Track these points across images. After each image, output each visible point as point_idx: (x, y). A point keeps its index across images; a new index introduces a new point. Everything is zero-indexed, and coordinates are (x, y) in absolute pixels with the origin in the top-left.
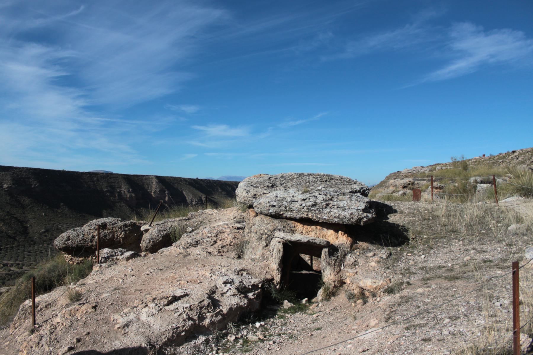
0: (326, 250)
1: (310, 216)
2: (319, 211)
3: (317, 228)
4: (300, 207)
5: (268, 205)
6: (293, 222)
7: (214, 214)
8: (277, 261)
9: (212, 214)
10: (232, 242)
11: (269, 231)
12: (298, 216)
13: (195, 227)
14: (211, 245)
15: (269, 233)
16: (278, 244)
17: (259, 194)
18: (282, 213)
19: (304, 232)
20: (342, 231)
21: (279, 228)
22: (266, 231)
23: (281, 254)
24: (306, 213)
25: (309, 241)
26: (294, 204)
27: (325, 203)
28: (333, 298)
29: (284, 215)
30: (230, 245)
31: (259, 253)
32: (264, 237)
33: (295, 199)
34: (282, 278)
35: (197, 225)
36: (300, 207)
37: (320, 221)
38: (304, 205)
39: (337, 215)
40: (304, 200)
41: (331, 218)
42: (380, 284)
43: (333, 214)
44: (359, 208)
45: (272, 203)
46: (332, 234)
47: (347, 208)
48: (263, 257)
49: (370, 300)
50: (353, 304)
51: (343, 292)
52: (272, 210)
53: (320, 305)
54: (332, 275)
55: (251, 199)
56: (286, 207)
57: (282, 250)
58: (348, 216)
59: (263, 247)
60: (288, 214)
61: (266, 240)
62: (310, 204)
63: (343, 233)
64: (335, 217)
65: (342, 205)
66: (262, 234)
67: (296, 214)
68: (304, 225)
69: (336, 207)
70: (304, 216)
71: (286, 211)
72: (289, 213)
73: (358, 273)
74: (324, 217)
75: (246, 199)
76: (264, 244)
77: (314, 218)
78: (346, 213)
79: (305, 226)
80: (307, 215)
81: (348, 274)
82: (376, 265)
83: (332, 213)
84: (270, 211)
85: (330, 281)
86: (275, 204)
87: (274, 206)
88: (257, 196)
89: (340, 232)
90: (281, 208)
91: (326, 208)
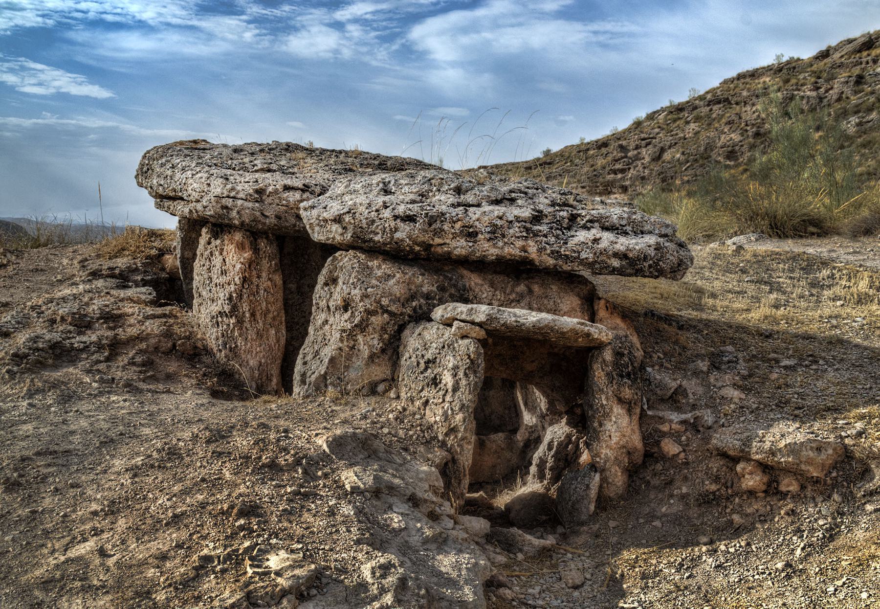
11: (395, 300)
15: (393, 308)
21: (425, 289)
22: (385, 302)
24: (520, 243)
32: (377, 320)
47: (629, 228)
58: (652, 252)
64: (616, 255)
72: (462, 242)
75: (229, 202)
80: (524, 249)
84: (398, 235)
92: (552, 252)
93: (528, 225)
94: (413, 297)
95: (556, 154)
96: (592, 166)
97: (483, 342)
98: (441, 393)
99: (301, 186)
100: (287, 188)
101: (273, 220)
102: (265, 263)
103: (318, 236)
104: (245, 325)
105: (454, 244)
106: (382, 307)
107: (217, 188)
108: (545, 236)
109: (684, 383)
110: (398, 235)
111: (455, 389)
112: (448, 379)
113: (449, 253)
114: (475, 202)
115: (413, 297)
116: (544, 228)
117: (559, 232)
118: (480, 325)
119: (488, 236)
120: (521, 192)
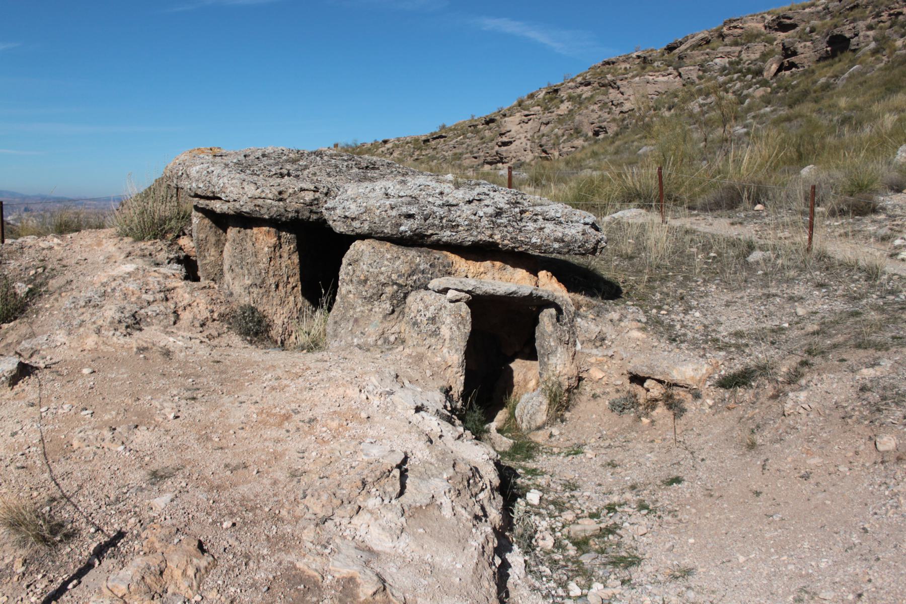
0: (553, 311)
1: (497, 237)
2: (513, 227)
3: (493, 266)
4: (473, 217)
5: (394, 213)
6: (445, 253)
7: (56, 248)
8: (462, 345)
9: (51, 248)
10: (212, 311)
12: (468, 238)
13: (30, 281)
14: (175, 323)
15: (400, 281)
16: (450, 306)
17: (291, 191)
18: (430, 232)
19: (470, 275)
20: (548, 271)
21: (422, 267)
22: (394, 277)
23: (468, 328)
24: (489, 232)
25: (531, 294)
26: (455, 213)
27: (517, 210)
28: (567, 415)
29: (435, 237)
30: (214, 320)
31: (372, 332)
32: (389, 290)
33: (452, 201)
34: (466, 384)
35: (36, 275)
36: (473, 217)
37: (520, 249)
38: (481, 214)
39: (560, 235)
40: (470, 202)
41: (547, 242)
42: (704, 371)
43: (537, 235)
44: (587, 220)
45: (404, 209)
46: (523, 278)
47: (562, 219)
48: (386, 341)
49: (690, 405)
50: (645, 421)
51: (584, 398)
52: (406, 227)
53: (555, 431)
54: (568, 365)
55: (274, 203)
56: (441, 218)
57: (469, 318)
59: (385, 317)
60: (446, 235)
61: (393, 297)
62: (490, 210)
63: (549, 274)
64: (556, 240)
65: (552, 214)
66: (384, 284)
67: (465, 234)
68: (467, 259)
69: (540, 217)
70: (484, 237)
71: (442, 227)
72: (448, 233)
73: (617, 357)
74: (534, 240)
75: (260, 202)
76: (388, 306)
77: (506, 242)
78: (574, 231)
79: (470, 262)
80: (491, 236)
81: (593, 360)
82: (644, 336)
83: (547, 231)
84: (402, 228)
85: (561, 379)
86: (413, 210)
87: (410, 216)
88: (285, 196)
89: (543, 274)
90: (430, 221)
91: (521, 220)
92: (512, 238)
93: (494, 219)
94: (413, 273)
95: (451, 130)
96: (482, 139)
97: (469, 303)
98: (441, 341)
99: (312, 188)
100: (302, 190)
101: (294, 214)
102: (285, 248)
103: (339, 228)
104: (271, 294)
105: (442, 233)
106: (392, 280)
107: (251, 190)
108: (506, 227)
109: (604, 329)
110: (402, 228)
111: (451, 339)
112: (445, 331)
113: (440, 240)
114: (454, 202)
115: (413, 273)
116: (504, 220)
117: (514, 224)
118: (468, 292)
119: (466, 228)
120: (485, 194)
